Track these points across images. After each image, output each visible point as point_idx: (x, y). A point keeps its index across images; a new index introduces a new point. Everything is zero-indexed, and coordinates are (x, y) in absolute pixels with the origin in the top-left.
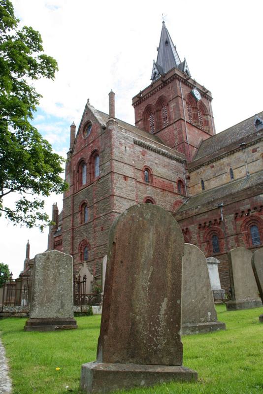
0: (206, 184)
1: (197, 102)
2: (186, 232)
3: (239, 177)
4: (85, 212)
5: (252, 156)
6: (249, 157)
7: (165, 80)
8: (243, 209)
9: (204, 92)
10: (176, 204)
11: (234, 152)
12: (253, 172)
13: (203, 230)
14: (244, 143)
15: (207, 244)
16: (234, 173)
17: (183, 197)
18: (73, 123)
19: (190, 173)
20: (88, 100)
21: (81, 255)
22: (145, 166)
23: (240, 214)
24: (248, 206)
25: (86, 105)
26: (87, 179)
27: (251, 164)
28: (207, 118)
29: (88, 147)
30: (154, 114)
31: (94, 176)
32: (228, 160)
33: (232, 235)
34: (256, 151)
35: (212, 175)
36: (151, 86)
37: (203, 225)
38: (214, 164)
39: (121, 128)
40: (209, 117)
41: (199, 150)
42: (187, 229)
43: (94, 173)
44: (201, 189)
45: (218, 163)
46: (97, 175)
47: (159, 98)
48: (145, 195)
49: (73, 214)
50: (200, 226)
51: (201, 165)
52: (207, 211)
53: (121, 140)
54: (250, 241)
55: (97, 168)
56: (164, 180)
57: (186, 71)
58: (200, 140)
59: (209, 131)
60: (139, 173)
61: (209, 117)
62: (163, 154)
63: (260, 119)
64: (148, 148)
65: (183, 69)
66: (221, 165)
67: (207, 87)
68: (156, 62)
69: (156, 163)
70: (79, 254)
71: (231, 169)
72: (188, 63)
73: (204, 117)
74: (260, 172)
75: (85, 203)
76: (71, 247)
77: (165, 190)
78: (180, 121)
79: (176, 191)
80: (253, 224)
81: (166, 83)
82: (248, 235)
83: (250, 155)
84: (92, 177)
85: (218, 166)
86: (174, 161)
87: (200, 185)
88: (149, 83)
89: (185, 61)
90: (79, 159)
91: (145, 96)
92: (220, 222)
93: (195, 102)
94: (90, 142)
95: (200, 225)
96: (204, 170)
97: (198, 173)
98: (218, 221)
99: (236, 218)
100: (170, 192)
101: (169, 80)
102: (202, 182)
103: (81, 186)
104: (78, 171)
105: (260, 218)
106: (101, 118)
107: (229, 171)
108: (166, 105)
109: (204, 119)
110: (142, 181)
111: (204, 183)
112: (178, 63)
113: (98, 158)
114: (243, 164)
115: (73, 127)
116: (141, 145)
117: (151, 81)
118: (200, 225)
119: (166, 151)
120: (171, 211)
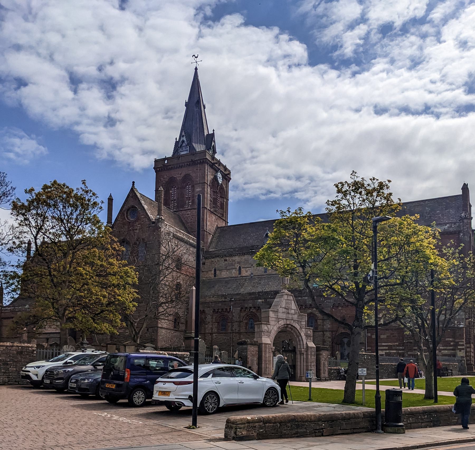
0: (218, 272)
11: (245, 255)
14: (254, 250)
16: (242, 271)
19: (205, 259)
23: (244, 309)
24: (251, 305)
30: (177, 189)
37: (216, 310)
45: (231, 259)
50: (214, 311)
71: (240, 267)
82: (247, 324)
87: (213, 272)
91: (170, 165)
92: (229, 311)
96: (218, 261)
98: (228, 310)
99: (241, 310)
105: (256, 314)
107: (238, 268)
114: (250, 266)
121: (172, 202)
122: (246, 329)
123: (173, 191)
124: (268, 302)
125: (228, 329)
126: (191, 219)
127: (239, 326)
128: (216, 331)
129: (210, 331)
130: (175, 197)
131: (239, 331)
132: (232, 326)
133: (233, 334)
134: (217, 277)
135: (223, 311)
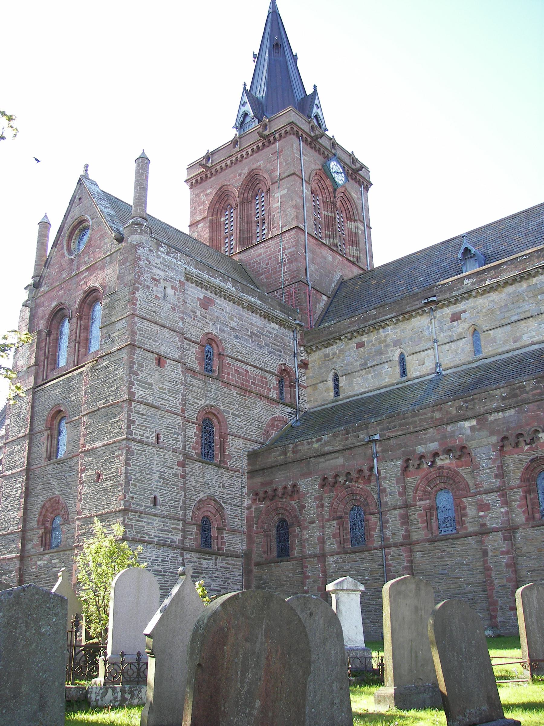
0: (343, 381)
1: (335, 190)
2: (292, 492)
3: (418, 374)
4: (60, 432)
5: (450, 329)
6: (442, 330)
7: (267, 133)
8: (424, 450)
9: (353, 167)
10: (273, 425)
11: (411, 317)
12: (452, 365)
13: (331, 491)
14: (434, 299)
15: (338, 524)
17: (289, 410)
18: (46, 216)
20: (87, 166)
21: (45, 533)
22: (208, 333)
24: (434, 446)
25: (80, 180)
26: (68, 355)
27: (447, 347)
28: (357, 228)
29: (76, 280)
30: (235, 209)
31: (87, 348)
32: (395, 333)
33: (395, 508)
34: (460, 318)
35: (358, 363)
36: (235, 142)
37: (331, 480)
38: (365, 339)
39: (159, 244)
40: (360, 226)
41: (331, 302)
42: (294, 486)
43: (87, 341)
44: (332, 394)
46: (94, 347)
47: (249, 173)
48: (203, 403)
49: (31, 436)
51: (335, 338)
52: (341, 448)
53: (156, 271)
54: (434, 524)
55: (96, 332)
56: (249, 368)
57: (316, 117)
58: (337, 277)
59: (358, 258)
60: (193, 350)
61: (360, 226)
62: (251, 308)
63: (470, 247)
64: (218, 291)
65: (312, 109)
66: (380, 343)
67: (362, 157)
68: (248, 88)
69: (232, 328)
70: (41, 532)
71: (402, 354)
72: (323, 98)
73: (351, 225)
74: (464, 367)
75: (60, 411)
76: (21, 513)
77: (250, 392)
78: (293, 232)
79: (274, 394)
80: (443, 485)
81: (269, 142)
83: (445, 327)
84: (82, 350)
85: (373, 345)
86: (273, 325)
87: (331, 384)
88: (231, 134)
89: (315, 93)
90: (54, 304)
92: (370, 476)
93: (331, 189)
94: (83, 268)
95: (325, 479)
96: (341, 351)
97: (326, 356)
98: (367, 473)
99: (405, 468)
100: (261, 396)
101: (277, 136)
102: (336, 380)
103: (54, 369)
104: (49, 334)
105: (458, 473)
106: (112, 213)
107: (396, 357)
108: (265, 191)
109: (349, 230)
110: (196, 366)
111: (340, 379)
112: (299, 96)
113: (98, 308)
114: (429, 345)
115: (45, 225)
116: (200, 284)
117: (235, 131)
118: (325, 479)
119: (258, 302)
120: (262, 441)
121: (227, 240)
122: (429, 527)
123: (227, 217)
124: (492, 422)
125: (372, 536)
126: (267, 264)
127: (406, 520)
128: (335, 546)
129: (317, 551)
130: (232, 228)
131: (408, 536)
132: (383, 523)
133: (387, 550)
134: (341, 396)
135: (351, 480)
